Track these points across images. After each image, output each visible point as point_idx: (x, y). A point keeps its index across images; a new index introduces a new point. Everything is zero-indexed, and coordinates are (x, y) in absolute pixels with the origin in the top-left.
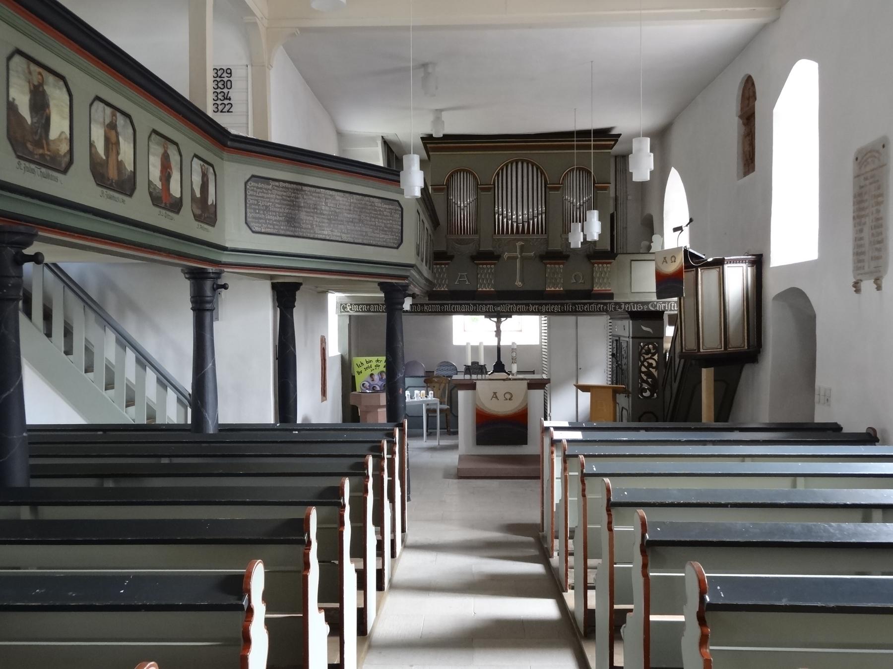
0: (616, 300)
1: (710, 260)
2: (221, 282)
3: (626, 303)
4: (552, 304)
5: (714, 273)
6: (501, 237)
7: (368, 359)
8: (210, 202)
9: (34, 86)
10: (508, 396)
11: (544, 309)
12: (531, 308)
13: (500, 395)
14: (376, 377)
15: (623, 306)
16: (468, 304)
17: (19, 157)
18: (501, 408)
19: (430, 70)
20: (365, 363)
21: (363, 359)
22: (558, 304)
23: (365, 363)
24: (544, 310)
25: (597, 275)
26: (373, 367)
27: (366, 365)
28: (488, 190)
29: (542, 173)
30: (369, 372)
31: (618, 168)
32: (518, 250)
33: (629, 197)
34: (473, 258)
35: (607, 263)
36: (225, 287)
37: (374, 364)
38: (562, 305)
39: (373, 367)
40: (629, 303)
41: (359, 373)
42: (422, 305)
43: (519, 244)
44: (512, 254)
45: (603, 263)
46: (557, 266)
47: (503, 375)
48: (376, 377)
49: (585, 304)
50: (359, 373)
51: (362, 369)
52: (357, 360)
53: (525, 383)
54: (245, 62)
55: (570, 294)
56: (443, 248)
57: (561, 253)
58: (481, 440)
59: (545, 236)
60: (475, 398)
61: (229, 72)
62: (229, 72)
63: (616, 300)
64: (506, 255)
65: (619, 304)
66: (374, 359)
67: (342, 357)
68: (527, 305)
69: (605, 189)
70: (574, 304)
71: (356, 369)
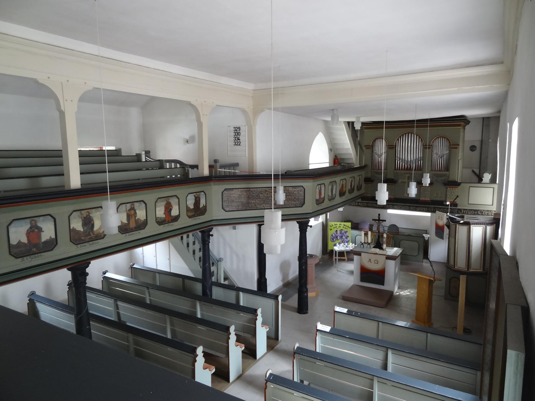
0: (458, 207)
1: (462, 222)
2: (211, 233)
3: (464, 210)
4: (422, 207)
5: (465, 228)
6: (398, 171)
8: (201, 206)
9: (84, 218)
10: (376, 262)
12: (412, 208)
13: (372, 261)
14: (338, 232)
17: (76, 245)
18: (373, 267)
19: (335, 112)
21: (333, 223)
22: (426, 207)
25: (448, 193)
27: (334, 226)
28: (392, 148)
29: (421, 140)
30: (335, 229)
31: (484, 123)
32: (407, 178)
33: (490, 140)
36: (212, 235)
37: (338, 226)
38: (428, 208)
40: (466, 210)
41: (331, 230)
42: (358, 202)
43: (407, 175)
44: (403, 180)
47: (377, 250)
48: (338, 232)
50: (331, 230)
51: (332, 228)
52: (330, 223)
53: (385, 257)
54: (245, 124)
56: (369, 175)
58: (363, 279)
60: (361, 260)
61: (239, 128)
62: (239, 128)
64: (400, 181)
65: (460, 210)
66: (338, 223)
67: (323, 222)
68: (410, 206)
69: (456, 148)
71: (329, 228)
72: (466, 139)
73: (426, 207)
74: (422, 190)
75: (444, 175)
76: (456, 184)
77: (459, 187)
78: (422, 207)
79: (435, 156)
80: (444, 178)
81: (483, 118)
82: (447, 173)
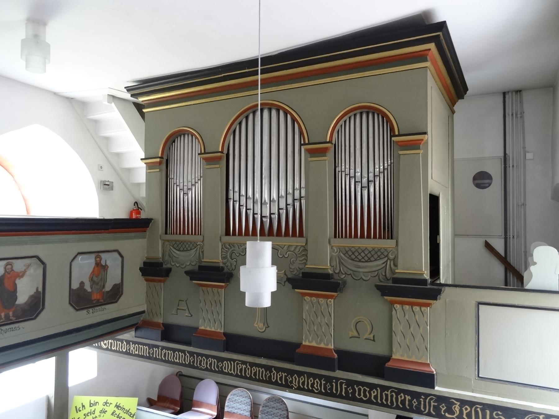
3: (463, 402)
7: (94, 399)
11: (295, 380)
12: (275, 376)
15: (457, 408)
16: (183, 351)
20: (87, 405)
23: (87, 405)
24: (295, 384)
25: (398, 328)
26: (97, 413)
27: (88, 409)
33: (529, 156)
34: (193, 275)
35: (421, 305)
38: (329, 380)
39: (97, 413)
40: (472, 404)
42: (128, 342)
45: (412, 304)
46: (322, 301)
49: (372, 386)
55: (348, 360)
56: (158, 254)
57: (327, 276)
59: (300, 242)
63: (439, 389)
66: (101, 400)
69: (415, 145)
70: (350, 383)
72: (457, 156)
73: (320, 377)
74: (306, 307)
75: (379, 254)
76: (423, 290)
77: (437, 304)
78: (310, 375)
79: (344, 181)
80: (377, 264)
81: (504, 94)
82: (388, 244)
